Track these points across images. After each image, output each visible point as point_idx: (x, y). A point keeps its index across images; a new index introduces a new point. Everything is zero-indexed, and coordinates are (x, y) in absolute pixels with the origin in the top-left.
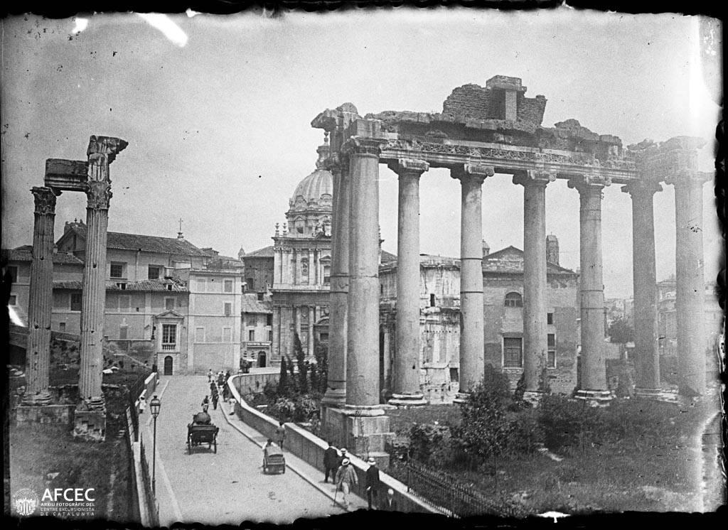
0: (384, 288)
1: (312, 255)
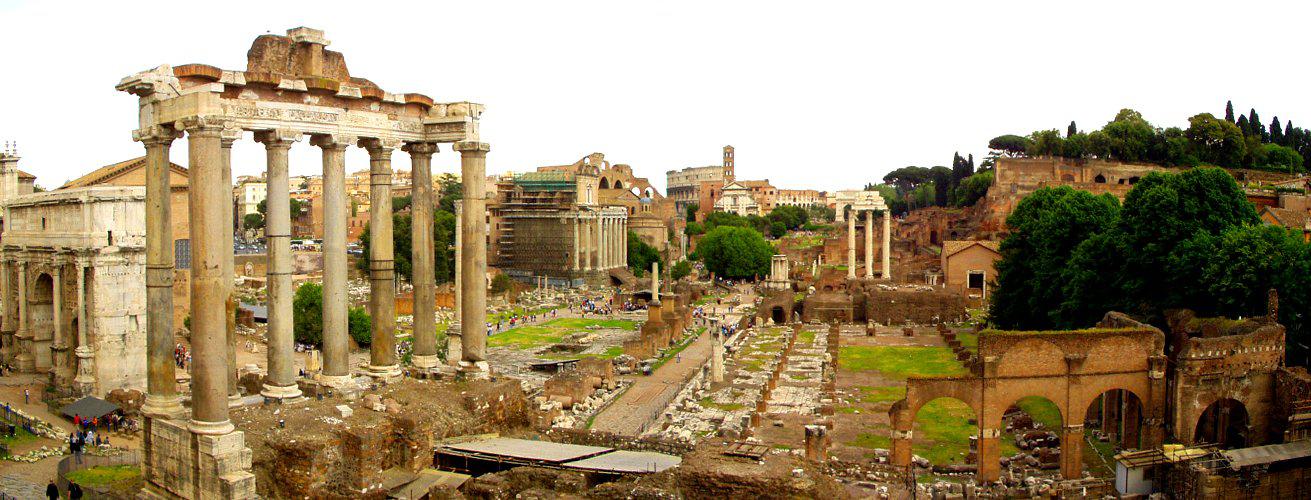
0: (47, 222)
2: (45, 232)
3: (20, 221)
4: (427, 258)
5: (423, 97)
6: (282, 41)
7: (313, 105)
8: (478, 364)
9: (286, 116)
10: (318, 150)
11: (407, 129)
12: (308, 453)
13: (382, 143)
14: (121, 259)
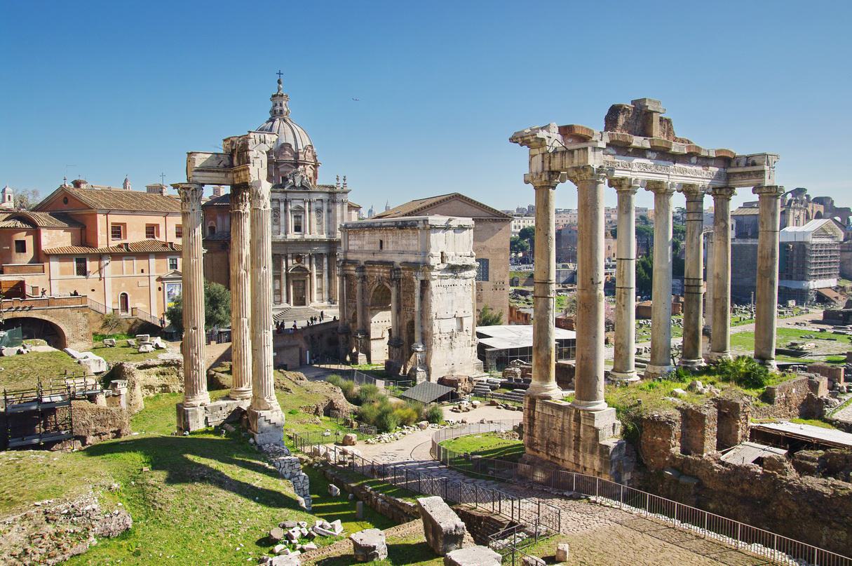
0: (385, 245)
1: (282, 205)
3: (357, 242)
5: (727, 151)
10: (651, 194)
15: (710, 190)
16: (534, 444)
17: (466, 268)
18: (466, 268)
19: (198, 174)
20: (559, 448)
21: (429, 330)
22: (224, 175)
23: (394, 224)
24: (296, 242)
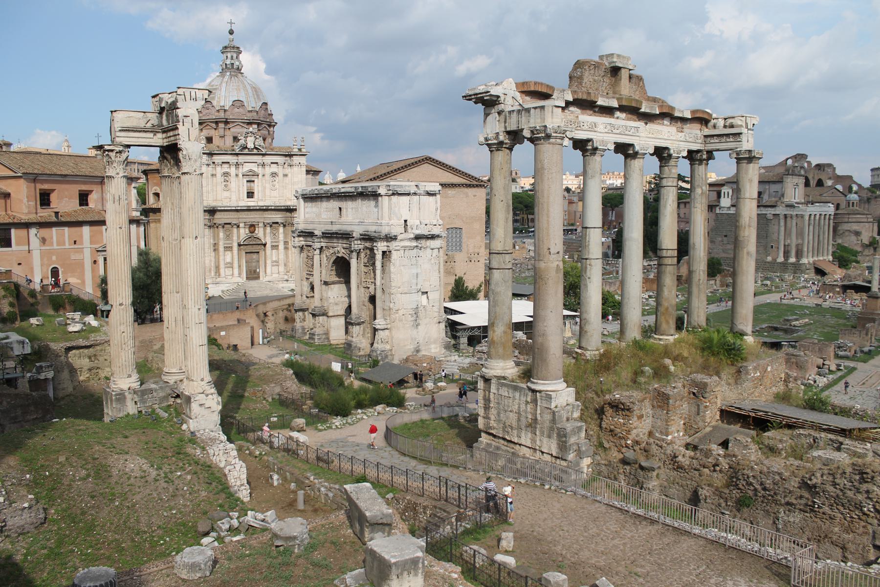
0: (344, 211)
1: (233, 169)
2: (344, 219)
4: (702, 248)
6: (597, 66)
7: (621, 120)
8: (745, 337)
9: (601, 128)
11: (690, 140)
12: (631, 406)
13: (672, 152)
14: (414, 244)
15: (685, 154)
16: (490, 428)
17: (433, 237)
18: (433, 237)
19: (123, 134)
20: (515, 432)
21: (392, 305)
22: (151, 135)
23: (353, 190)
24: (249, 210)
